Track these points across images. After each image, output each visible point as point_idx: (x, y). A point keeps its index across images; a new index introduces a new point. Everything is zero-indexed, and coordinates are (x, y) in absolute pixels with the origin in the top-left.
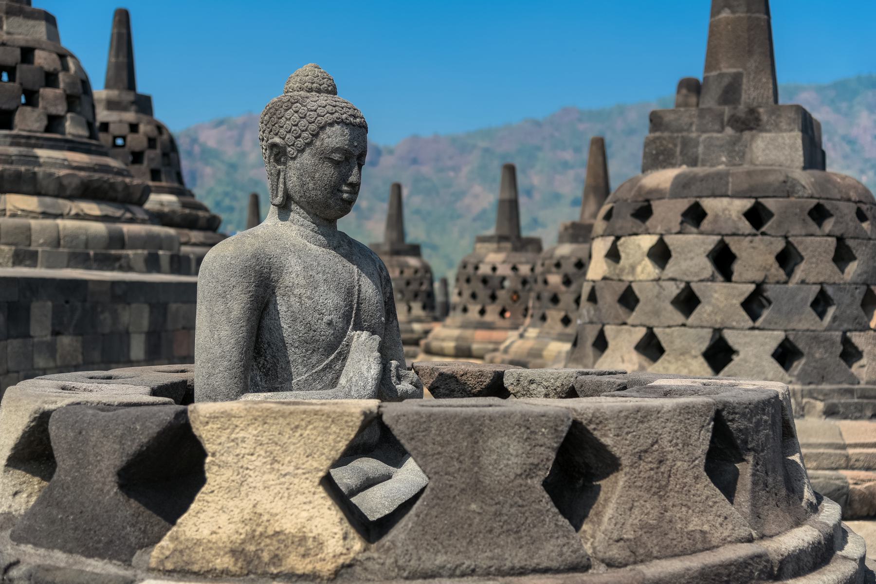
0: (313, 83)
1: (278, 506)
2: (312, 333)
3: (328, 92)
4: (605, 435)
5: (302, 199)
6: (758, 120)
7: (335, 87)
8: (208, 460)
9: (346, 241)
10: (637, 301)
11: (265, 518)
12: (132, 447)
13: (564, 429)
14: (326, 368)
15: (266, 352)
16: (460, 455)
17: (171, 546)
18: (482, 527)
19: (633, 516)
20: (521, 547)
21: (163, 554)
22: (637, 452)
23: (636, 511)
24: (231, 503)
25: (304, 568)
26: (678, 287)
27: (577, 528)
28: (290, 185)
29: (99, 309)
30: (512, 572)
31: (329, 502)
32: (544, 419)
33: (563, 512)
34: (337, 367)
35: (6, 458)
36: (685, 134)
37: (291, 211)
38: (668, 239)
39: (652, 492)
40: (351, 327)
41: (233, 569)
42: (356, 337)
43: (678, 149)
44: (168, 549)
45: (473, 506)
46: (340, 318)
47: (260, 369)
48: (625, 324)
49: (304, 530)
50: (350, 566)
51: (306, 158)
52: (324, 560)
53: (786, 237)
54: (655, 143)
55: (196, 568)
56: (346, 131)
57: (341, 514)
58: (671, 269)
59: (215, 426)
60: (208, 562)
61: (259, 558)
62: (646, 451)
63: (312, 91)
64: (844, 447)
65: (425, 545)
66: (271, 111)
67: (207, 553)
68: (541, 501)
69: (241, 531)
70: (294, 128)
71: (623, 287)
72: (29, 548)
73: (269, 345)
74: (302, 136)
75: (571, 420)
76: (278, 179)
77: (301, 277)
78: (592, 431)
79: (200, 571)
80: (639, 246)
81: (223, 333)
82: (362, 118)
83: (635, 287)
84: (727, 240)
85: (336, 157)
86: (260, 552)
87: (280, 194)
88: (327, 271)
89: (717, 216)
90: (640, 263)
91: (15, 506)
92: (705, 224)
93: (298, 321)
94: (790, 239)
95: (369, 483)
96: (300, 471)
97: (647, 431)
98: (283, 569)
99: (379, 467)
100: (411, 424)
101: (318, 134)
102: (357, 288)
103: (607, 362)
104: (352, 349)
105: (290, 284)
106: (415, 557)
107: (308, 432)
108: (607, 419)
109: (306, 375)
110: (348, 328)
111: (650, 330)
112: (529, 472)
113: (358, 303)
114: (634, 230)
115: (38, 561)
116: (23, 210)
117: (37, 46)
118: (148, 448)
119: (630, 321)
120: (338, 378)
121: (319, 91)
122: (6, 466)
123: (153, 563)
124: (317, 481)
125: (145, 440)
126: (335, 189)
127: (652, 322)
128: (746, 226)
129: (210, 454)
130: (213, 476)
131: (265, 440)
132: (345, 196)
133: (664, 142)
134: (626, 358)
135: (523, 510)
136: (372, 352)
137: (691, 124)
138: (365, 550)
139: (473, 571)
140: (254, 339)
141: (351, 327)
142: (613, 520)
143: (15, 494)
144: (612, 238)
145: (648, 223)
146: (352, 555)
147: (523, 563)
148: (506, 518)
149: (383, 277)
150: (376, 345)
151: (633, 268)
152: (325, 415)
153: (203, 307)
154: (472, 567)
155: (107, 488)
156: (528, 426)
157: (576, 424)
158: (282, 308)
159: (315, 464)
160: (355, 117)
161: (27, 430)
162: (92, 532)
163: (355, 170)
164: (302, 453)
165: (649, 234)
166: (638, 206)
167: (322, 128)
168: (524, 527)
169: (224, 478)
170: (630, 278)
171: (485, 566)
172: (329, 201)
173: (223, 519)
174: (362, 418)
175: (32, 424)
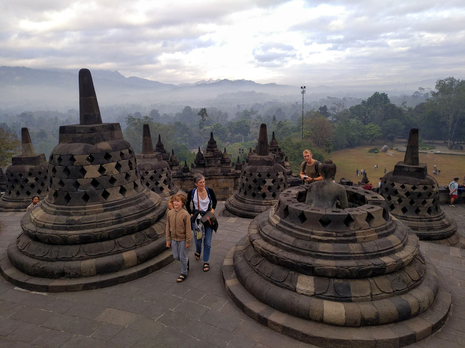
36: (101, 133)
38: (120, 162)
43: (101, 137)
71: (109, 178)
90: (114, 170)
111: (122, 187)
127: (122, 184)
134: (118, 195)
151: (112, 172)
170: (112, 175)
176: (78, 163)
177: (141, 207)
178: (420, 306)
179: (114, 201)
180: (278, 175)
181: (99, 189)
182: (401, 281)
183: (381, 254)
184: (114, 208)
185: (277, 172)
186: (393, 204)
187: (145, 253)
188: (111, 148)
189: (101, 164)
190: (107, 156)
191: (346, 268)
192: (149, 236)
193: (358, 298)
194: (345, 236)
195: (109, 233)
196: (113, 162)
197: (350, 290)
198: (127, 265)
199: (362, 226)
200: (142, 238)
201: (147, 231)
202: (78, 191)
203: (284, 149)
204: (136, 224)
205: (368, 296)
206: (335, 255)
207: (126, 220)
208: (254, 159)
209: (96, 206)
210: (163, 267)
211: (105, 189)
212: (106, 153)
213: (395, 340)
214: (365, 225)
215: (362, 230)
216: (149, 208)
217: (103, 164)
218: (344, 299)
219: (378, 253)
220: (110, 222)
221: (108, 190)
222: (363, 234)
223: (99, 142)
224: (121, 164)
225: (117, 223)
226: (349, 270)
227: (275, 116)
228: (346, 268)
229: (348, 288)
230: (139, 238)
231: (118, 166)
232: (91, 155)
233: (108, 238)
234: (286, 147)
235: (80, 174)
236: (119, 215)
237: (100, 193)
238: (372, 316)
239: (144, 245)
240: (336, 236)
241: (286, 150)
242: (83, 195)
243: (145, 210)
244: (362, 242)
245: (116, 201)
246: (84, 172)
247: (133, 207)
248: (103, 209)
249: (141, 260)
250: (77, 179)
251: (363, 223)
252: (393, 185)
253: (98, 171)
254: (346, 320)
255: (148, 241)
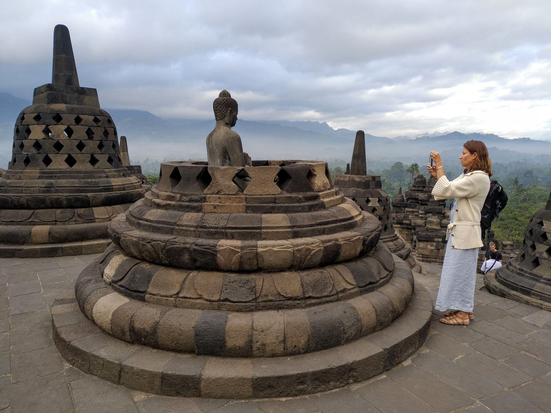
6: (85, 92)
26: (78, 142)
38: (71, 127)
43: (60, 98)
48: (59, 153)
53: (105, 128)
58: (74, 136)
64: (133, 183)
71: (55, 142)
83: (61, 142)
84: (91, 128)
89: (86, 120)
92: (82, 123)
94: (106, 128)
103: (52, 166)
111: (69, 155)
119: (60, 153)
128: (94, 124)
137: (63, 90)
144: (45, 125)
151: (59, 136)
176: (26, 122)
177: (87, 183)
178: (251, 336)
179: (53, 169)
180: (368, 201)
181: (40, 153)
182: (247, 287)
183: (226, 233)
184: (51, 176)
185: (368, 198)
186: (537, 258)
187: (61, 231)
188: (65, 109)
189: (47, 126)
190: (58, 118)
191: (149, 242)
192: (81, 215)
193: (155, 297)
194: (191, 201)
195: (27, 200)
196: (62, 124)
197: (149, 282)
198: (34, 239)
199: (223, 187)
200: (69, 215)
201: (81, 211)
202: (22, 153)
203: (517, 220)
204: (64, 197)
205: (171, 296)
206: (155, 225)
207: (57, 191)
208: (342, 179)
209: (33, 172)
210: (81, 254)
211: (47, 154)
212: (58, 114)
213: (152, 375)
214: (229, 187)
215: (221, 195)
216: (100, 187)
217: (49, 125)
218: (135, 294)
219: (223, 230)
220: (36, 189)
221: (50, 156)
222: (219, 200)
223: (56, 103)
224: (73, 129)
225: (44, 192)
226: (151, 245)
227: (517, 178)
228: (149, 242)
229: (148, 278)
230: (64, 215)
231: (69, 131)
232: (40, 114)
233: (28, 207)
234: (519, 218)
235: (26, 134)
236: (52, 184)
237: (41, 157)
238: (145, 327)
239: (69, 224)
240: (180, 200)
241: (519, 222)
242: (25, 158)
243: (91, 187)
244: (211, 212)
245: (58, 169)
246: (29, 131)
247: (76, 180)
248: (38, 175)
249: (53, 238)
250: (23, 141)
251: (227, 183)
252: (541, 224)
253: (42, 131)
254: (111, 324)
255: (77, 221)
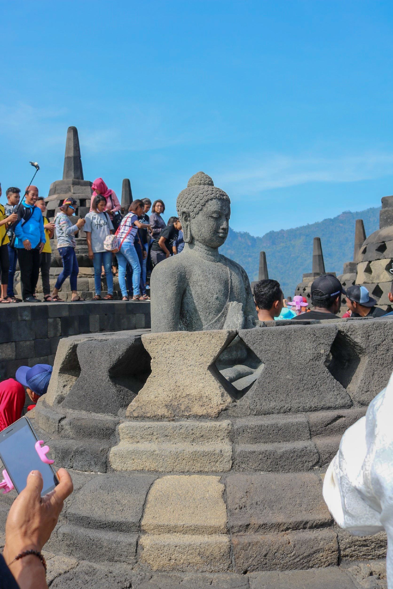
0: (201, 181)
1: (188, 382)
2: (208, 304)
3: (209, 184)
4: (357, 337)
5: (200, 238)
7: (212, 182)
8: (152, 361)
9: (223, 258)
10: (382, 292)
11: (181, 388)
12: (115, 357)
13: (334, 335)
14: (217, 321)
15: (186, 315)
16: (280, 350)
17: (136, 405)
18: (294, 387)
19: (374, 379)
20: (314, 397)
21: (132, 409)
22: (375, 346)
23: (376, 376)
24: (164, 381)
25: (202, 412)
27: (345, 387)
28: (193, 232)
29: (121, 317)
30: (310, 409)
31: (213, 378)
32: (323, 330)
33: (335, 378)
34: (222, 321)
35: (59, 369)
37: (195, 245)
39: (384, 366)
40: (228, 300)
41: (166, 414)
42: (230, 305)
44: (134, 406)
45: (288, 377)
46: (222, 296)
47: (184, 324)
49: (201, 393)
50: (226, 409)
51: (200, 217)
52: (212, 408)
54: (385, 213)
55: (149, 415)
56: (219, 203)
57: (219, 384)
59: (154, 344)
60: (154, 412)
61: (179, 408)
62: (379, 345)
63: (201, 185)
65: (264, 397)
66: (181, 196)
67: (154, 407)
68: (324, 372)
69: (170, 395)
70: (193, 203)
72: (70, 411)
73: (188, 312)
74: (197, 206)
75: (338, 330)
76: (187, 229)
77: (201, 277)
78: (349, 336)
79: (150, 416)
80: (381, 265)
81: (164, 306)
82: (227, 196)
85: (215, 215)
86: (179, 405)
87: (189, 236)
88: (214, 273)
91: (64, 392)
93: (201, 298)
95: (240, 376)
96: (198, 363)
97: (379, 334)
98: (191, 413)
99: (246, 369)
100: (253, 336)
101: (205, 204)
102: (230, 280)
104: (229, 311)
105: (196, 280)
106: (259, 404)
107: (200, 343)
108: (356, 329)
109: (207, 325)
110: (226, 300)
112: (317, 357)
113: (230, 288)
114: (378, 257)
115: (74, 416)
116: (85, 274)
117: (87, 198)
118: (122, 357)
120: (223, 326)
121: (205, 184)
122: (59, 373)
123: (128, 414)
124: (207, 367)
125: (120, 353)
126: (216, 232)
129: (152, 358)
130: (155, 369)
131: (179, 349)
132: (221, 235)
133: (390, 212)
135: (315, 377)
136: (239, 311)
138: (233, 402)
139: (290, 409)
140: (179, 308)
141: (228, 300)
142: (363, 381)
143: (64, 386)
145: (384, 253)
146: (226, 404)
147: (316, 405)
148: (306, 382)
149: (244, 276)
150: (241, 307)
151: (378, 277)
152: (209, 334)
153: (153, 294)
154: (289, 408)
155: (104, 378)
156: (315, 334)
157: (340, 332)
158: (193, 293)
159: (205, 360)
160: (223, 195)
161: (67, 354)
162: (99, 400)
163: (225, 223)
164: (198, 354)
165: (385, 258)
166: (379, 245)
167: (207, 201)
168: (315, 386)
169: (160, 369)
171: (296, 407)
172: (213, 238)
173: (160, 390)
174: (228, 334)
175: (70, 351)
